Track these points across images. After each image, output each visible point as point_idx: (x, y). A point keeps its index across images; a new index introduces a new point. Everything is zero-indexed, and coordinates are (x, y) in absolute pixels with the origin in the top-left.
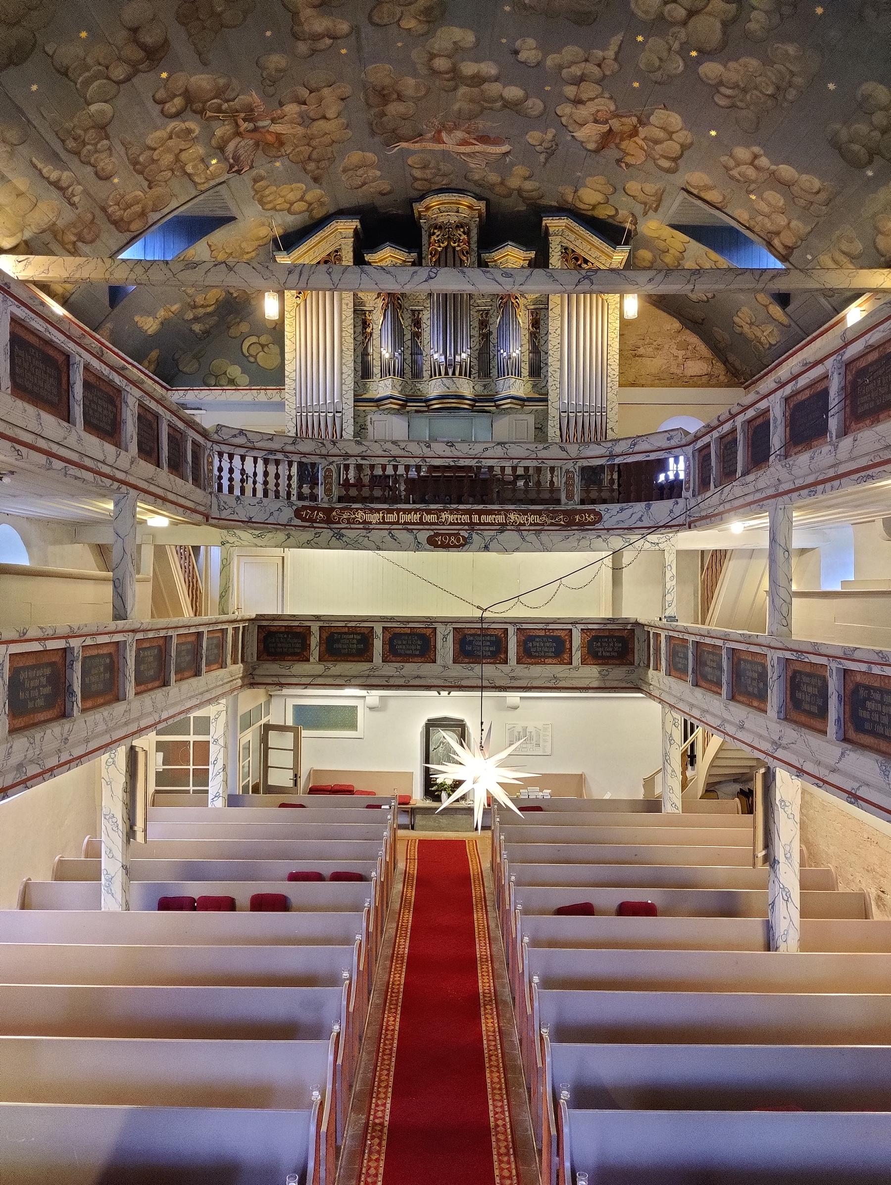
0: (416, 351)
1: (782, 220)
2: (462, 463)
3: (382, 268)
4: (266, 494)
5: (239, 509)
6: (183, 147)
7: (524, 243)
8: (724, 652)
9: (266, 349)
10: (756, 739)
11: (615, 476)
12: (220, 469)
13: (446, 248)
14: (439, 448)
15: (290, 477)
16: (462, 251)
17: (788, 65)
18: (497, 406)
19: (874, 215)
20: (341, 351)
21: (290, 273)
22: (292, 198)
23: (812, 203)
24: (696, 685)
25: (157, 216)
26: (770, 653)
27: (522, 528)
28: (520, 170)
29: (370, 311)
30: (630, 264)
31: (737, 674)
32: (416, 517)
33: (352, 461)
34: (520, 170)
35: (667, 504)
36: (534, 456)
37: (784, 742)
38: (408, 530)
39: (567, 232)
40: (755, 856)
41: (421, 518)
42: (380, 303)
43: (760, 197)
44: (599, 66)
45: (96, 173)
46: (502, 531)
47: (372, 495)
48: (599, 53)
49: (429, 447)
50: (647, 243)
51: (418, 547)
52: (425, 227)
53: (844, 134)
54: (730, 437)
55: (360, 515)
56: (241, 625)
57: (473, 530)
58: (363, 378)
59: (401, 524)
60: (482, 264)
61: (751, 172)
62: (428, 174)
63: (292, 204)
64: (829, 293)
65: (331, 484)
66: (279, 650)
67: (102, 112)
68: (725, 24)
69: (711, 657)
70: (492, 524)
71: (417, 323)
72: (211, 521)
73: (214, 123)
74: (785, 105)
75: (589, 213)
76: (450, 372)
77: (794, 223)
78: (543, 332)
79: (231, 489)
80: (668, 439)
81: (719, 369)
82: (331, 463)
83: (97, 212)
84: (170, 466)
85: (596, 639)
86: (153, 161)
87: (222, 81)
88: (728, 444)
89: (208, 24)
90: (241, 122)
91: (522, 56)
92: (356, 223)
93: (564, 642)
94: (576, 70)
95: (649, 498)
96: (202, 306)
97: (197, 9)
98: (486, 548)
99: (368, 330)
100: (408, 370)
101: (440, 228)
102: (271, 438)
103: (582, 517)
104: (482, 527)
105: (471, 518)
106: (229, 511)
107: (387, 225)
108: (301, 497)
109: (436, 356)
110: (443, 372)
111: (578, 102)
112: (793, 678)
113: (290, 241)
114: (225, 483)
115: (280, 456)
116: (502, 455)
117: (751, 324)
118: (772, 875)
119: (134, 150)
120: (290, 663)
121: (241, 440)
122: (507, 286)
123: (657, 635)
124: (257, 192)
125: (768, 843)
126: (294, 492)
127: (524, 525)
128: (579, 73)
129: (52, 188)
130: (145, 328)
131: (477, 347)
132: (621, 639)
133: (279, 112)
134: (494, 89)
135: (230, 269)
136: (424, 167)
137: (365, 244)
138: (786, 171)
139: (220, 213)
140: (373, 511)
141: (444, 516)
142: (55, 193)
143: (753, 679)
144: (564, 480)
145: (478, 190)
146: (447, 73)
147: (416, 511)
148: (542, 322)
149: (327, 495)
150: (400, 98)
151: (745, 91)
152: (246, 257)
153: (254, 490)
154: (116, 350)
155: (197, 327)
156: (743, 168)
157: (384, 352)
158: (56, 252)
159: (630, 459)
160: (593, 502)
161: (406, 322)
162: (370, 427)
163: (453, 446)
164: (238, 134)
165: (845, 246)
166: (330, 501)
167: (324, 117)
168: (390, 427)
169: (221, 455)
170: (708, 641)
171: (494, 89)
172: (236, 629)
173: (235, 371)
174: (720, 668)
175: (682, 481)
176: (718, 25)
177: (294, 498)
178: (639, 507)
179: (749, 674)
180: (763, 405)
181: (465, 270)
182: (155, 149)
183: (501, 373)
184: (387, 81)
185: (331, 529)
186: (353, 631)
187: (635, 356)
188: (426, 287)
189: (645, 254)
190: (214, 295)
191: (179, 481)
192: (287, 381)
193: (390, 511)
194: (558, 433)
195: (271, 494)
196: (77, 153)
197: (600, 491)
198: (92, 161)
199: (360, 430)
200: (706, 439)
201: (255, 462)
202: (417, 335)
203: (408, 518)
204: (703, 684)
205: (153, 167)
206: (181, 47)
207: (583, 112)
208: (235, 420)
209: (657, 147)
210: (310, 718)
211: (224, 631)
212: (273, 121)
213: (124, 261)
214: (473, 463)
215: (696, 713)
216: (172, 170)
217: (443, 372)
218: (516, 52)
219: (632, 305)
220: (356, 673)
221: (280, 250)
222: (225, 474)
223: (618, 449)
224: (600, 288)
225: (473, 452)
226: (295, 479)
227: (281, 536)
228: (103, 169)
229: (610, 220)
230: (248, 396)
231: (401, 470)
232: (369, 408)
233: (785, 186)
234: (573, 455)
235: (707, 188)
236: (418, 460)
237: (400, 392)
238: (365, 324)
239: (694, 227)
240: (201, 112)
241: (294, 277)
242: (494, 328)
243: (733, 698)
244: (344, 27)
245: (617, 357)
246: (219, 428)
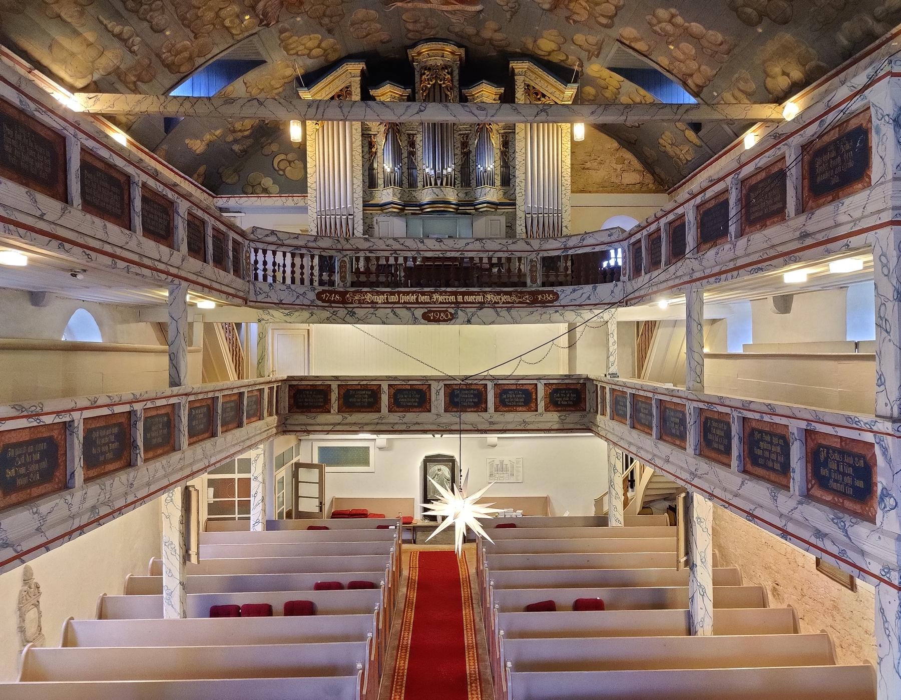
0: (412, 166)
1: (694, 65)
2: (449, 255)
3: (383, 103)
4: (293, 281)
5: (272, 294)
7: (495, 80)
8: (653, 402)
9: (292, 164)
10: (679, 470)
11: (569, 263)
12: (256, 262)
13: (434, 85)
14: (431, 244)
15: (312, 268)
16: (447, 87)
18: (476, 209)
19: (764, 62)
20: (352, 166)
21: (309, 107)
22: (311, 45)
24: (633, 427)
25: (202, 60)
26: (687, 403)
28: (492, 25)
29: (375, 135)
30: (578, 99)
31: (663, 419)
32: (413, 298)
33: (361, 254)
34: (492, 25)
35: (609, 286)
36: (505, 249)
37: (699, 473)
39: (529, 73)
40: (678, 562)
41: (417, 299)
42: (382, 128)
43: (677, 47)
45: (152, 28)
46: (481, 308)
47: (377, 280)
49: (423, 242)
50: (592, 81)
51: (415, 321)
52: (417, 68)
54: (655, 235)
55: (369, 297)
56: (275, 385)
58: (369, 187)
60: (463, 99)
61: (669, 28)
62: (419, 26)
63: (311, 50)
64: (730, 122)
65: (345, 272)
66: (306, 404)
69: (644, 405)
70: (473, 303)
71: (412, 144)
72: (249, 303)
75: (546, 58)
76: (439, 182)
77: (703, 67)
78: (511, 151)
79: (265, 278)
80: (609, 235)
81: (649, 178)
82: (345, 256)
83: (154, 58)
84: (214, 261)
85: (556, 391)
86: (198, 17)
88: (654, 240)
92: (361, 66)
93: (531, 394)
95: (595, 282)
96: (240, 131)
98: (469, 322)
99: (374, 150)
100: (405, 181)
101: (429, 69)
102: (297, 237)
105: (456, 299)
107: (387, 66)
108: (321, 283)
109: (427, 170)
110: (433, 183)
112: (705, 423)
113: (310, 79)
114: (260, 273)
115: (304, 251)
116: (480, 248)
117: (672, 144)
118: (692, 577)
120: (314, 414)
121: (272, 239)
122: (482, 118)
123: (603, 388)
124: (282, 41)
125: (688, 552)
126: (316, 278)
127: (498, 303)
130: (194, 148)
131: (460, 163)
132: (576, 391)
135: (261, 104)
136: (415, 22)
137: (369, 81)
139: (253, 57)
140: (379, 293)
141: (435, 296)
142: (117, 44)
143: (675, 423)
144: (529, 267)
145: (458, 40)
147: (413, 293)
152: (276, 91)
153: (284, 278)
154: (171, 167)
155: (236, 148)
157: (386, 167)
158: (121, 90)
159: (580, 251)
160: (552, 285)
161: (403, 143)
162: (376, 226)
165: (742, 85)
166: (344, 286)
168: (392, 227)
169: (256, 251)
170: (641, 393)
172: (271, 389)
173: (267, 182)
174: (651, 415)
175: (620, 267)
177: (316, 284)
178: (588, 288)
179: (673, 419)
180: (680, 211)
181: (448, 104)
182: (199, 8)
183: (479, 183)
186: (365, 388)
187: (584, 168)
188: (417, 118)
189: (590, 90)
190: (248, 124)
191: (222, 273)
192: (309, 190)
193: (392, 294)
194: (524, 230)
195: (298, 281)
196: (135, 12)
197: (557, 276)
199: (368, 229)
200: (638, 236)
201: (284, 256)
202: (412, 154)
204: (639, 427)
208: (267, 222)
210: (331, 457)
211: (261, 391)
213: (175, 97)
214: (457, 255)
215: (633, 449)
216: (214, 25)
217: (433, 183)
219: (580, 131)
220: (368, 422)
221: (302, 86)
222: (260, 266)
223: (571, 243)
224: (554, 118)
225: (457, 246)
226: (317, 268)
227: (306, 314)
229: (563, 64)
230: (278, 202)
231: (401, 261)
232: (375, 211)
233: (696, 39)
234: (536, 248)
235: (636, 40)
237: (400, 199)
238: (371, 145)
239: (626, 70)
241: (312, 110)
242: (472, 148)
243: (660, 438)
245: (569, 170)
246: (255, 229)
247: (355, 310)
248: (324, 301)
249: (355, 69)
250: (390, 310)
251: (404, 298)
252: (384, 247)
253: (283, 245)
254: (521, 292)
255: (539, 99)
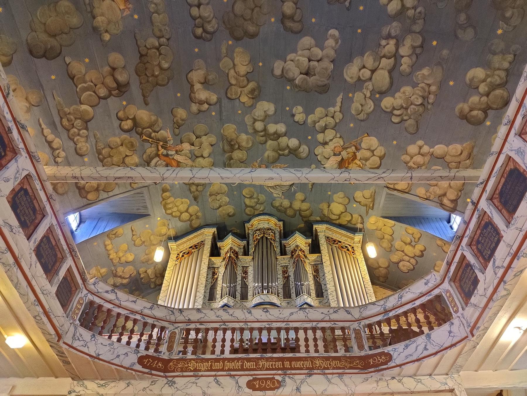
6: (128, 154)
13: (262, 237)
17: (425, 81)
23: (460, 162)
27: (327, 371)
29: (218, 268)
36: (327, 318)
38: (230, 376)
41: (242, 366)
44: (333, 117)
46: (310, 375)
48: (332, 109)
49: (250, 313)
53: (466, 108)
57: (285, 374)
59: (225, 371)
63: (181, 213)
67: (86, 111)
68: (390, 72)
70: (301, 369)
73: (147, 145)
74: (429, 107)
78: (321, 274)
82: (176, 328)
87: (153, 118)
89: (150, 79)
90: (160, 148)
91: (297, 118)
92: (214, 230)
94: (322, 123)
97: (146, 69)
99: (216, 276)
103: (375, 360)
104: (293, 372)
105: (283, 365)
106: (82, 343)
111: (325, 144)
115: (138, 317)
119: (101, 145)
124: (164, 199)
128: (324, 125)
129: (46, 144)
133: (180, 147)
134: (284, 141)
138: (439, 149)
146: (262, 132)
148: (320, 270)
149: (169, 351)
150: (239, 148)
151: (406, 109)
156: (415, 158)
163: (267, 311)
164: (157, 155)
167: (202, 156)
171: (284, 141)
176: (387, 74)
184: (234, 136)
185: (166, 377)
198: (75, 139)
205: (109, 159)
206: (135, 90)
207: (328, 150)
209: (367, 163)
212: (177, 152)
218: (293, 116)
228: (80, 149)
236: (241, 324)
240: (141, 134)
244: (214, 98)
247: (176, 379)
248: (144, 366)
250: (213, 378)
251: (228, 365)
252: (214, 318)
253: (119, 307)
254: (350, 357)
255: (337, 244)
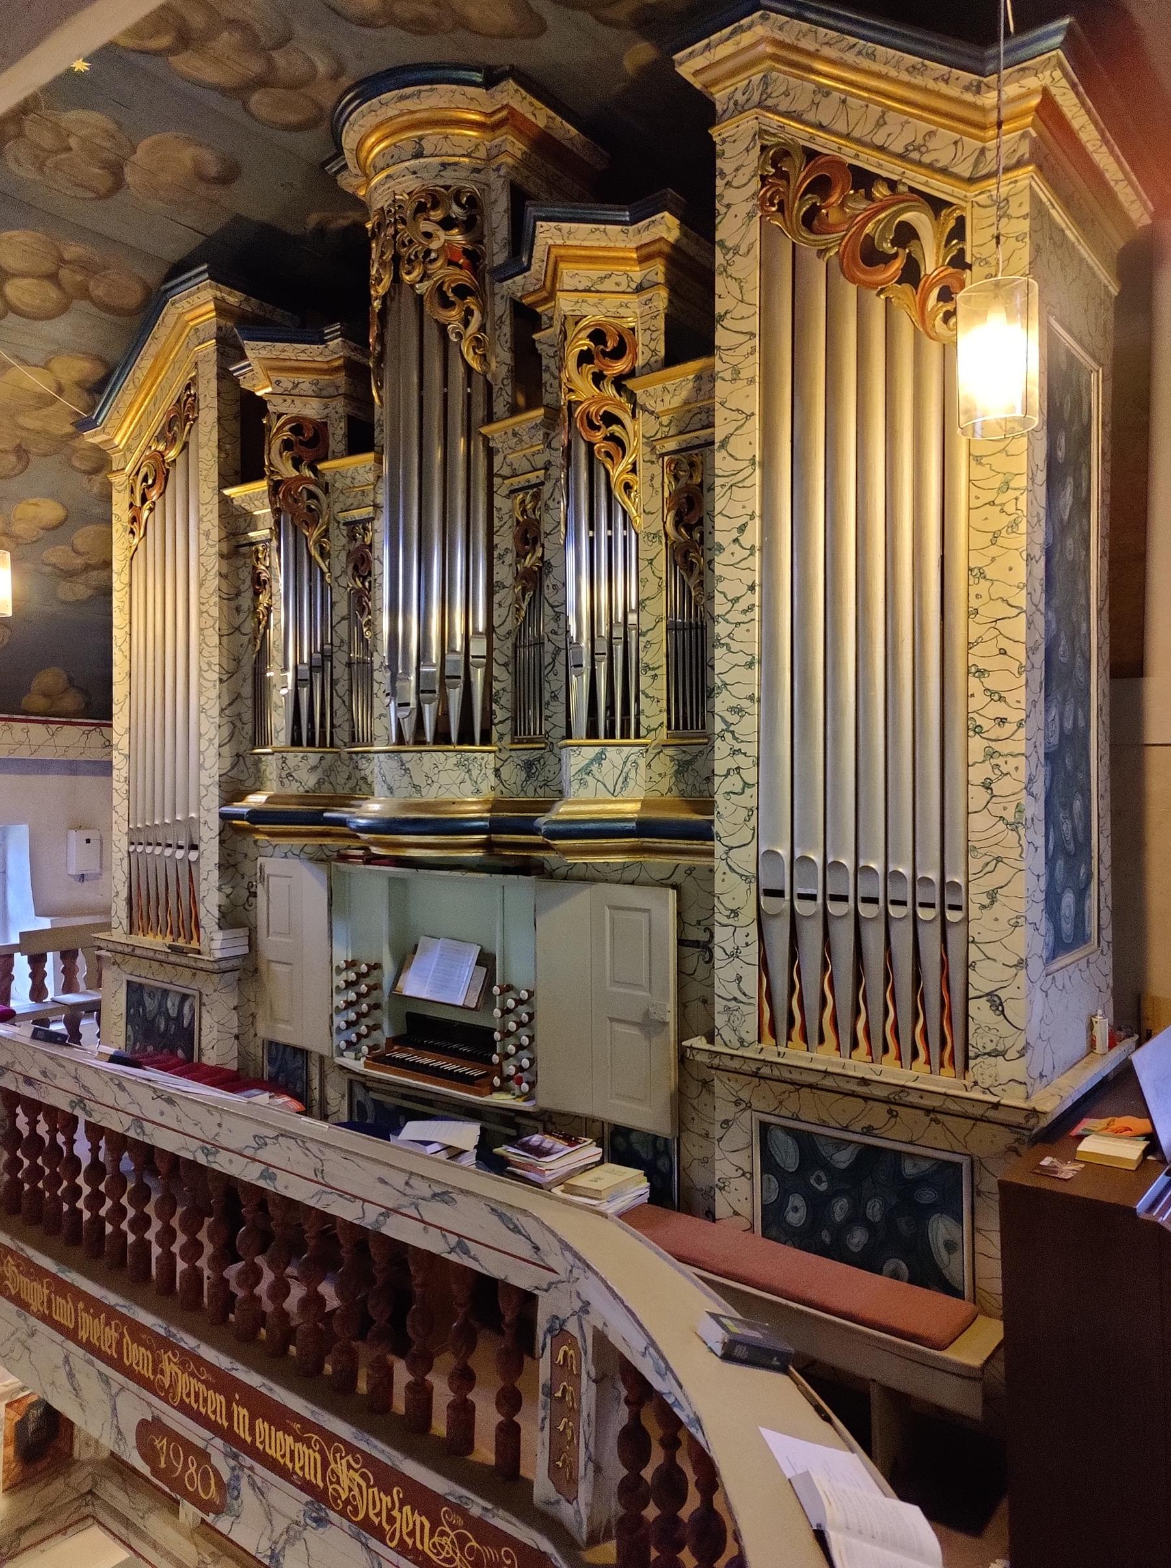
203: (92, 1328)
249: (198, 307)
